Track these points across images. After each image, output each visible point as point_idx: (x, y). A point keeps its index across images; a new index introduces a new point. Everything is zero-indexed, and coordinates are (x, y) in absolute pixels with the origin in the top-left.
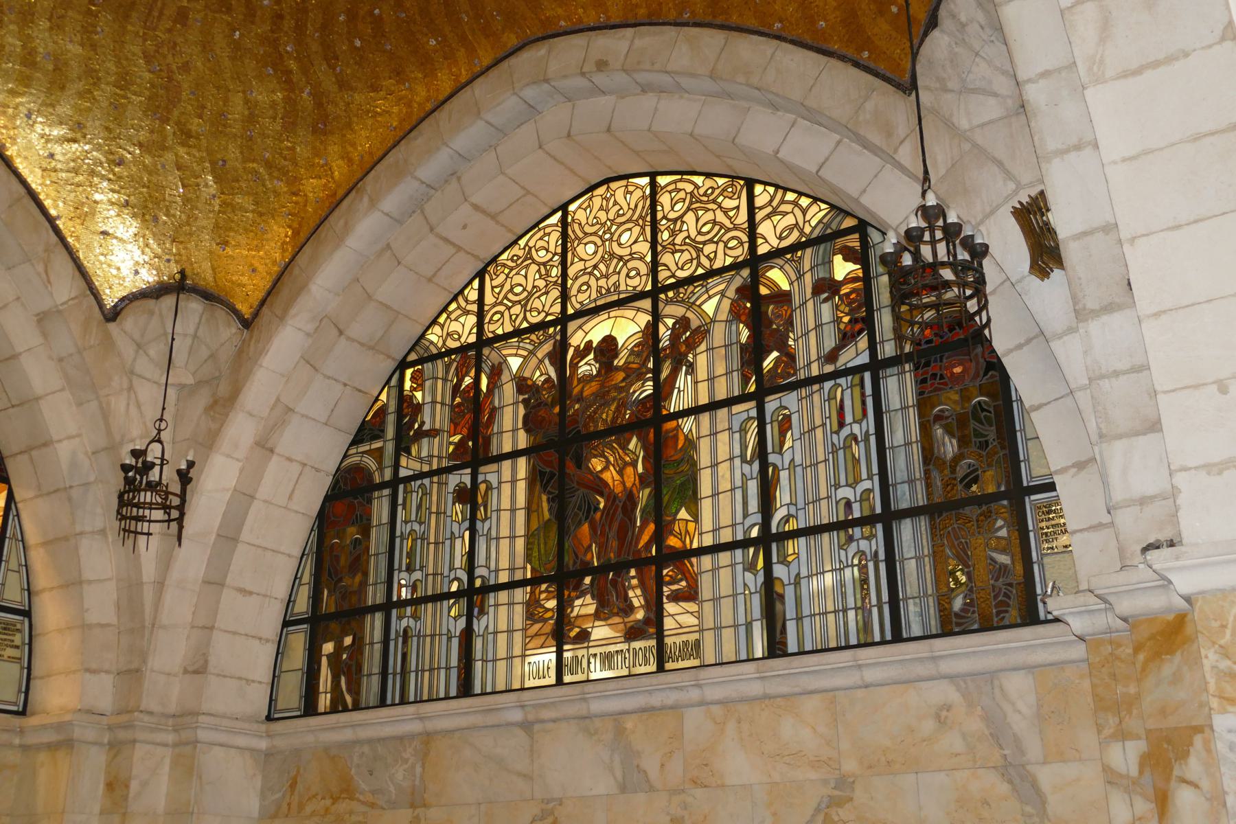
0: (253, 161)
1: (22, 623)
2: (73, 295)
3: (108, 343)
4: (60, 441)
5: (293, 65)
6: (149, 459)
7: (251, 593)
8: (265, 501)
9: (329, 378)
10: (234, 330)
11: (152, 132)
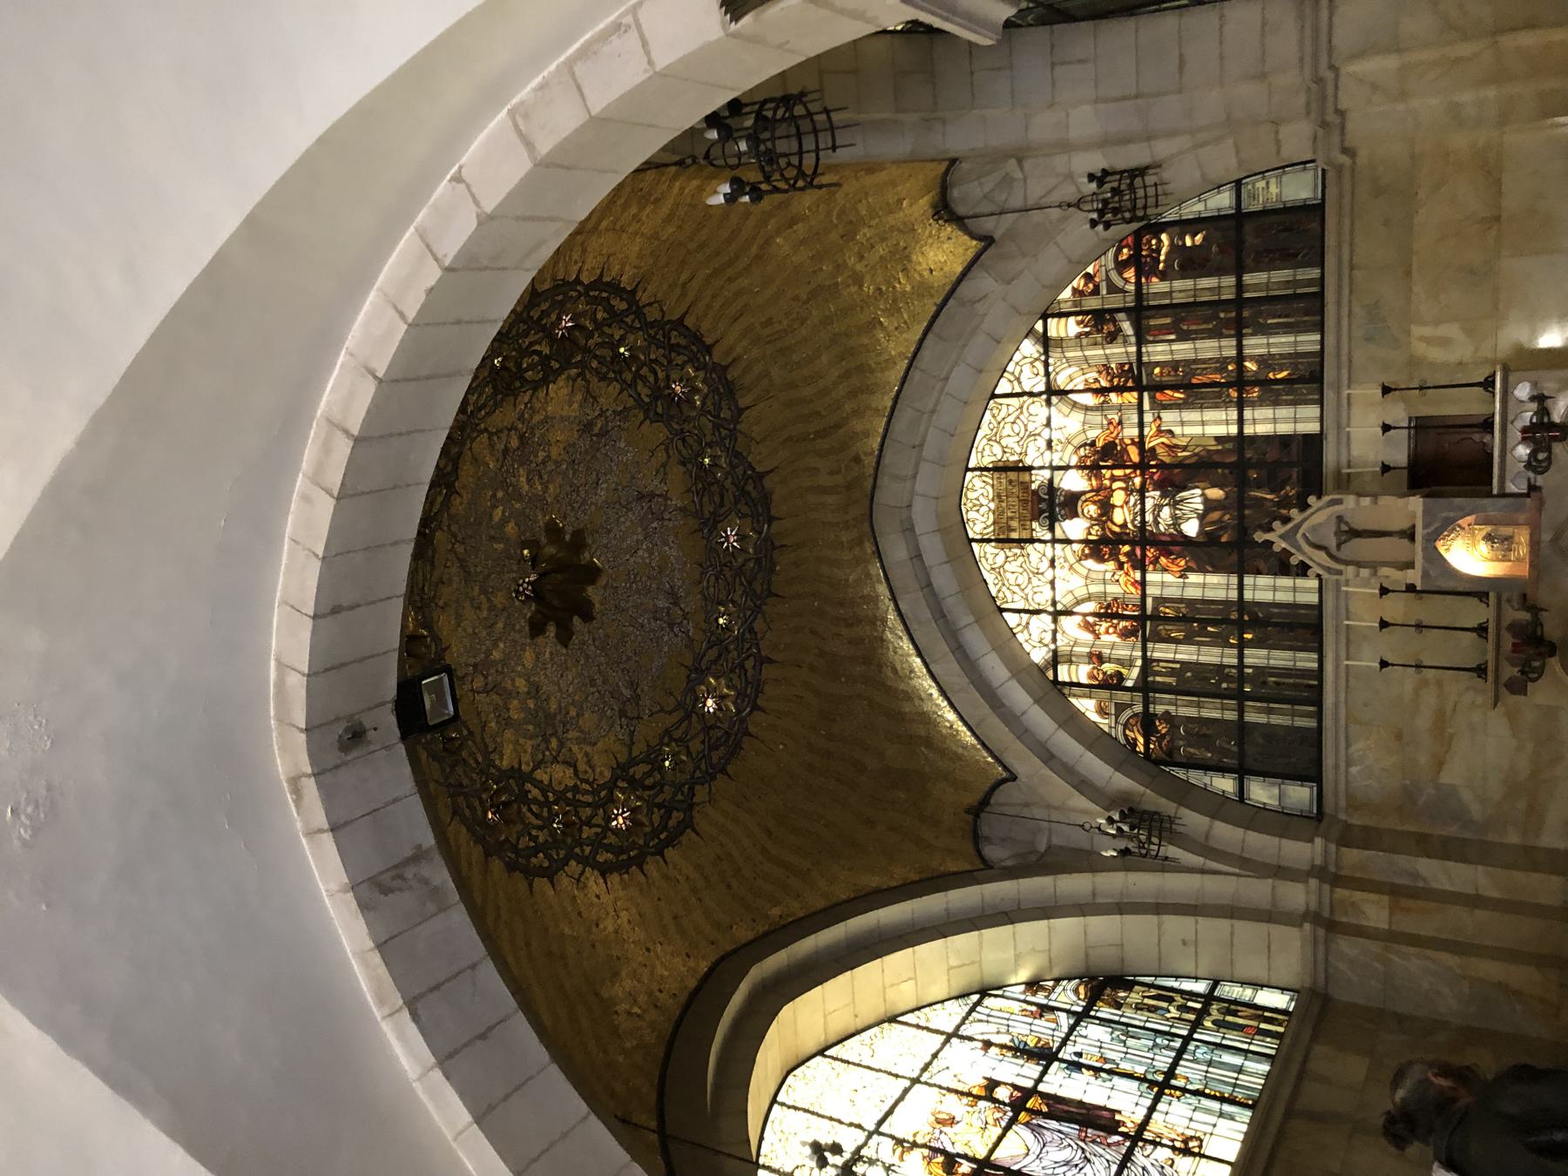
0: (832, 221)
1: (1247, 183)
2: (987, 275)
7: (1181, 55)
8: (1096, 86)
9: (973, 94)
10: (963, 164)
11: (848, 286)
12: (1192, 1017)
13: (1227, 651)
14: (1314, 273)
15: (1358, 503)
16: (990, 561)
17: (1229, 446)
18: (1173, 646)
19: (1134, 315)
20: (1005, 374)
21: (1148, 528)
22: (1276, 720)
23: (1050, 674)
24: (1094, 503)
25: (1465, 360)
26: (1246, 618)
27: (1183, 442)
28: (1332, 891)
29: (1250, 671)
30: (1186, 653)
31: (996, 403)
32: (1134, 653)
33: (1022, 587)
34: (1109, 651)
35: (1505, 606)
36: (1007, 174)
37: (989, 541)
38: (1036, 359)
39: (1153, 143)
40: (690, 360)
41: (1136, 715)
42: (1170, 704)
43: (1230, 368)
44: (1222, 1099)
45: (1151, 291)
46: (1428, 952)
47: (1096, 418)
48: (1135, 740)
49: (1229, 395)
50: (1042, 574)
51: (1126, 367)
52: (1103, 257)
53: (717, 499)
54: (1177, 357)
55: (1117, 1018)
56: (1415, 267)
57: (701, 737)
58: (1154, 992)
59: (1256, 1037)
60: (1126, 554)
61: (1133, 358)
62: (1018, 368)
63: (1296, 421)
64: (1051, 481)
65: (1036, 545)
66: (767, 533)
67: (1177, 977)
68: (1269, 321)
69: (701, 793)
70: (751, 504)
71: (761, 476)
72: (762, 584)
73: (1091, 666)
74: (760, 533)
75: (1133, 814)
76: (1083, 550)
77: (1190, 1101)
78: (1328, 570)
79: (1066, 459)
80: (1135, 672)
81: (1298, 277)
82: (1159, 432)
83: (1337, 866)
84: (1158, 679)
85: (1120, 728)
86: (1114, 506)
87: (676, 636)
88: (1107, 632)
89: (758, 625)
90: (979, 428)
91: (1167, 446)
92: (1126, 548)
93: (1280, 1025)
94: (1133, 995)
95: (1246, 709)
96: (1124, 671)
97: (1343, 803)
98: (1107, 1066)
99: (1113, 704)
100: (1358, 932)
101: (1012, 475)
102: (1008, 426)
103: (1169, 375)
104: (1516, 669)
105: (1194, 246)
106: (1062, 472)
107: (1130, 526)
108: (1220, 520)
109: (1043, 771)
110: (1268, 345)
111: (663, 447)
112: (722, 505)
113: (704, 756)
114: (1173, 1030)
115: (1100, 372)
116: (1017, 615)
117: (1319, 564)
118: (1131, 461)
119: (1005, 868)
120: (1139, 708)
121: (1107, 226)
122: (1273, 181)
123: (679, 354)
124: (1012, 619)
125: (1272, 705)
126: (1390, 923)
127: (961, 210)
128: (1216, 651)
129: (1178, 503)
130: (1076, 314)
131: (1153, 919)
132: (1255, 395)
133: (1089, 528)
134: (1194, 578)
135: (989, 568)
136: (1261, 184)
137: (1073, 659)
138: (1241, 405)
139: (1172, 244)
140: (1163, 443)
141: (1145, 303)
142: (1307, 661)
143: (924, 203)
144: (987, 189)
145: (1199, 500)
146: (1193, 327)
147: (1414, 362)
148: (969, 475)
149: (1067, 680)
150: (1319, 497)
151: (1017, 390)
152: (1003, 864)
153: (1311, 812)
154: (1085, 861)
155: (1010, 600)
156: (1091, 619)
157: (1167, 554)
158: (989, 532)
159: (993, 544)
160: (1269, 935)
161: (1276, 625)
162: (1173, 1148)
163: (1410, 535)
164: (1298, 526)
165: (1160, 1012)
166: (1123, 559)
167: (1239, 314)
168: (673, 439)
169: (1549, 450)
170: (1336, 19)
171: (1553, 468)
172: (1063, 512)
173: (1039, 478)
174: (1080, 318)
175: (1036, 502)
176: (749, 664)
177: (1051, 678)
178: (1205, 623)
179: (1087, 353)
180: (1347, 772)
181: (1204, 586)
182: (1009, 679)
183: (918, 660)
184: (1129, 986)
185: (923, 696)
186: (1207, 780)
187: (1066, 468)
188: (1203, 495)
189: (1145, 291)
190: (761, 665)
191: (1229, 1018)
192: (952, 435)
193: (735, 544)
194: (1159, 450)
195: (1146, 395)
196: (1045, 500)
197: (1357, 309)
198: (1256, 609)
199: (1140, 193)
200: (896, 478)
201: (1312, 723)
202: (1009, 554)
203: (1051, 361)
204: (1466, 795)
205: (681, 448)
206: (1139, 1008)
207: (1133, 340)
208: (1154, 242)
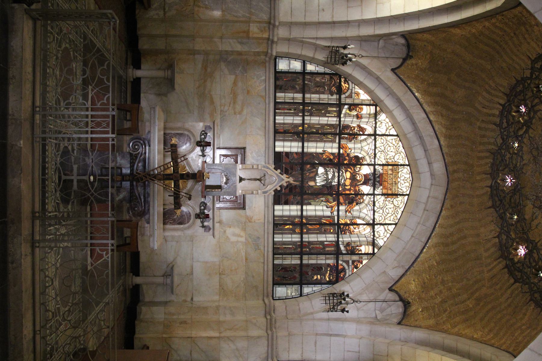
1: (298, 295)
3: (383, 290)
4: (350, 286)
5: (481, 304)
6: (347, 299)
7: (316, 346)
10: (396, 321)
11: (447, 280)
14: (276, 262)
16: (401, 156)
17: (306, 202)
18: (329, 123)
19: (339, 252)
20: (390, 233)
21: (336, 170)
22: (291, 95)
23: (378, 109)
24: (358, 180)
25: (229, 228)
26: (301, 135)
28: (269, 36)
29: (300, 114)
30: (324, 120)
31: (395, 222)
32: (344, 119)
33: (388, 146)
34: (354, 120)
36: (381, 313)
37: (401, 165)
38: (378, 238)
39: (328, 317)
40: (515, 264)
41: (344, 93)
42: (331, 99)
43: (305, 230)
45: (333, 260)
46: (235, 19)
47: (355, 214)
48: (345, 83)
50: (379, 151)
51: (343, 233)
52: (350, 274)
53: (513, 201)
54: (324, 235)
56: (244, 261)
57: (527, 97)
60: (346, 160)
61: (340, 236)
62: (385, 235)
63: (283, 210)
64: (374, 190)
65: (381, 163)
66: (493, 181)
68: (291, 246)
69: (528, 73)
70: (499, 195)
71: (493, 206)
72: (497, 159)
73: (361, 113)
74: (496, 182)
75: (344, 60)
76: (362, 161)
78: (268, 168)
79: (368, 198)
81: (281, 261)
83: (268, 43)
84: (335, 109)
85: (351, 88)
86: (350, 179)
87: (536, 143)
88: (354, 127)
89: (500, 141)
90: (403, 212)
91: (328, 202)
92: (346, 162)
95: (301, 99)
96: (348, 112)
97: (267, 64)
99: (353, 97)
101: (390, 192)
102: (390, 212)
104: (209, 134)
105: (317, 275)
106: (369, 193)
107: (344, 171)
108: (310, 173)
109: (380, 73)
111: (532, 229)
112: (511, 197)
113: (526, 88)
115: (353, 231)
116: (391, 134)
117: (271, 170)
118: (343, 197)
119: (395, 35)
120: (343, 96)
121: (343, 293)
122: (289, 295)
123: (519, 268)
124: (393, 132)
125: (292, 101)
127: (400, 303)
128: (312, 122)
129: (325, 180)
130: (362, 254)
131: (335, 19)
133: (360, 170)
134: (320, 151)
135: (402, 154)
136: (293, 294)
137: (368, 116)
138: (302, 216)
139: (325, 276)
141: (335, 256)
142: (280, 119)
143: (413, 308)
144: (389, 309)
145: (318, 181)
146: (318, 246)
148: (408, 193)
149: (371, 107)
151: (386, 226)
152: (397, 36)
154: (363, 40)
155: (393, 140)
156: (361, 133)
157: (330, 160)
158: (401, 169)
159: (399, 164)
161: (291, 133)
163: (241, 179)
164: (278, 183)
166: (347, 158)
167: (302, 250)
168: (528, 231)
169: (200, 210)
170: (266, 349)
172: (370, 177)
173: (378, 191)
174: (360, 252)
175: (381, 181)
176: (505, 125)
177: (378, 107)
179: (358, 239)
180: (266, 76)
181: (316, 148)
182: (393, 110)
183: (431, 118)
185: (430, 104)
186: (317, 69)
187: (368, 195)
188: (316, 183)
189: (335, 260)
190: (500, 123)
192: (411, 213)
193: (508, 178)
194: (332, 201)
195: (336, 222)
196: (377, 182)
197: (262, 248)
199: (331, 301)
200: (436, 198)
201: (278, 95)
202: (392, 159)
203: (372, 237)
204: (226, 71)
205: (525, 226)
207: (340, 243)
208: (331, 278)
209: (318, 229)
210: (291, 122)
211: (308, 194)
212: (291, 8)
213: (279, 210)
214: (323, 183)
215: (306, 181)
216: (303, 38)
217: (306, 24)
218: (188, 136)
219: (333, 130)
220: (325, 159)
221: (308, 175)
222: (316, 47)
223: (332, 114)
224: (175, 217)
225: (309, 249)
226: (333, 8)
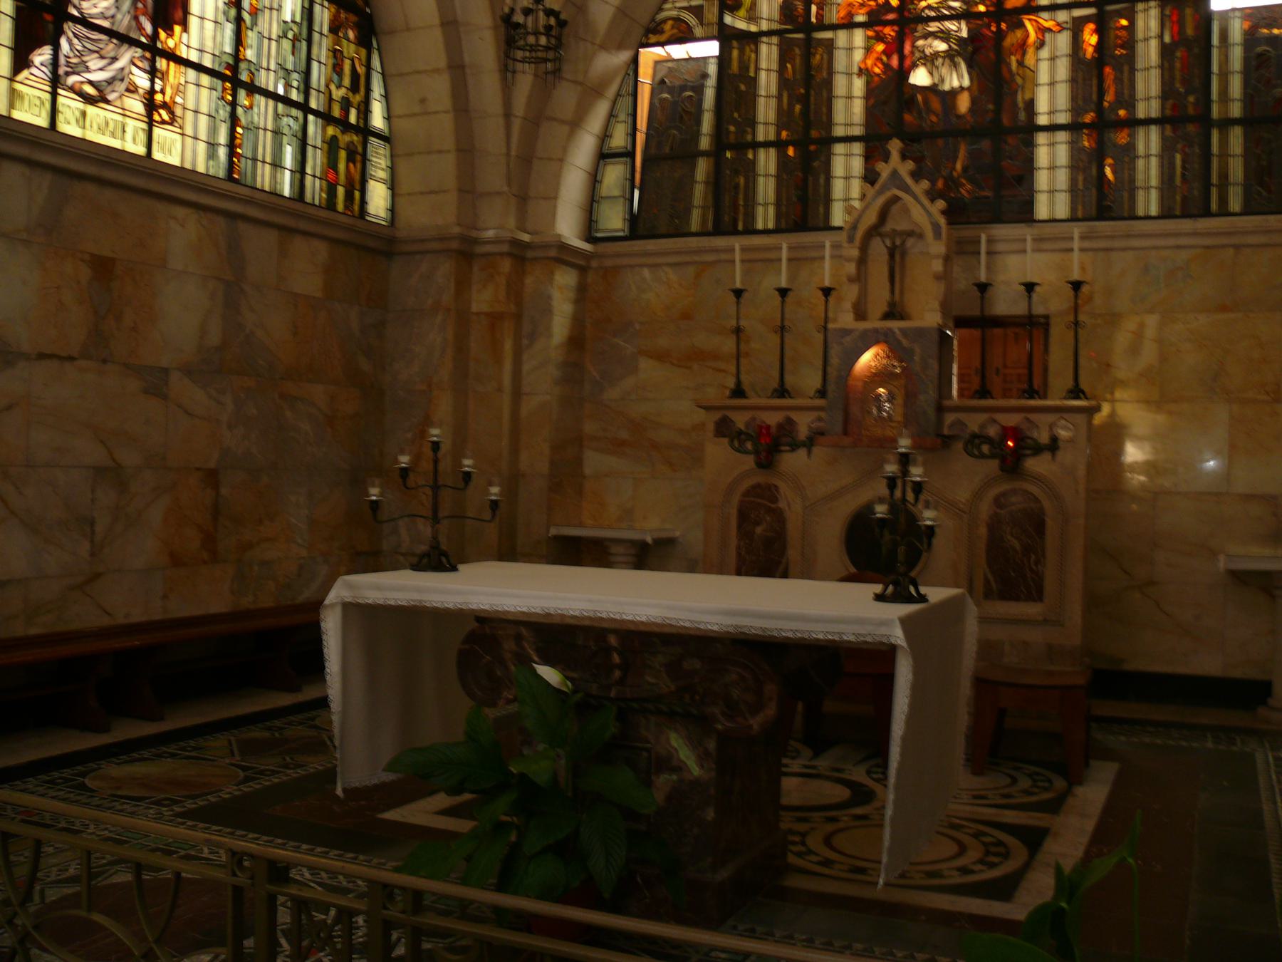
12: (336, 112)
13: (772, 130)
14: (1235, 204)
15: (937, 257)
17: (1022, 116)
18: (775, 66)
26: (812, 148)
27: (1029, 60)
28: (501, 254)
29: (750, 156)
30: (767, 82)
35: (814, 415)
41: (690, 28)
44: (232, 146)
48: (662, 32)
49: (1087, 112)
54: (1140, 47)
55: (316, 28)
58: (361, 70)
59: (324, 183)
63: (1052, 192)
67: (386, 96)
77: (221, 112)
80: (741, 25)
82: (1042, 30)
85: (674, 13)
93: (346, 207)
94: (353, 47)
96: (742, 12)
97: (609, 263)
98: (246, 16)
100: (462, 284)
103: (1117, 37)
108: (929, 110)
110: (1148, 156)
114: (313, 93)
126: (478, 314)
128: (772, 117)
129: (952, 60)
131: (442, 63)
132: (1086, 144)
134: (859, 85)
138: (1073, 127)
140: (1028, 36)
145: (956, 84)
147: (1113, 319)
150: (943, 212)
153: (597, 231)
160: (445, 191)
161: (805, 180)
162: (152, 92)
163: (894, 312)
164: (907, 189)
165: (335, 77)
167: (1189, 119)
169: (992, 456)
171: (971, 459)
178: (805, 100)
181: (850, 97)
184: (364, 42)
186: (622, 117)
188: (962, 88)
191: (343, 154)
197: (1184, 255)
198: (823, 159)
206: (336, 54)
209: (1118, 68)
210: (772, 183)
211: (998, 111)
212: (422, 193)
213: (1052, 203)
214: (963, 67)
215: (954, 120)
216: (508, 154)
217: (467, 151)
218: (747, 493)
219: (797, 51)
220: (887, 67)
221: (937, 116)
222: (536, 119)
223: (749, 57)
224: (1016, 544)
225: (1187, 93)
226: (419, 72)
